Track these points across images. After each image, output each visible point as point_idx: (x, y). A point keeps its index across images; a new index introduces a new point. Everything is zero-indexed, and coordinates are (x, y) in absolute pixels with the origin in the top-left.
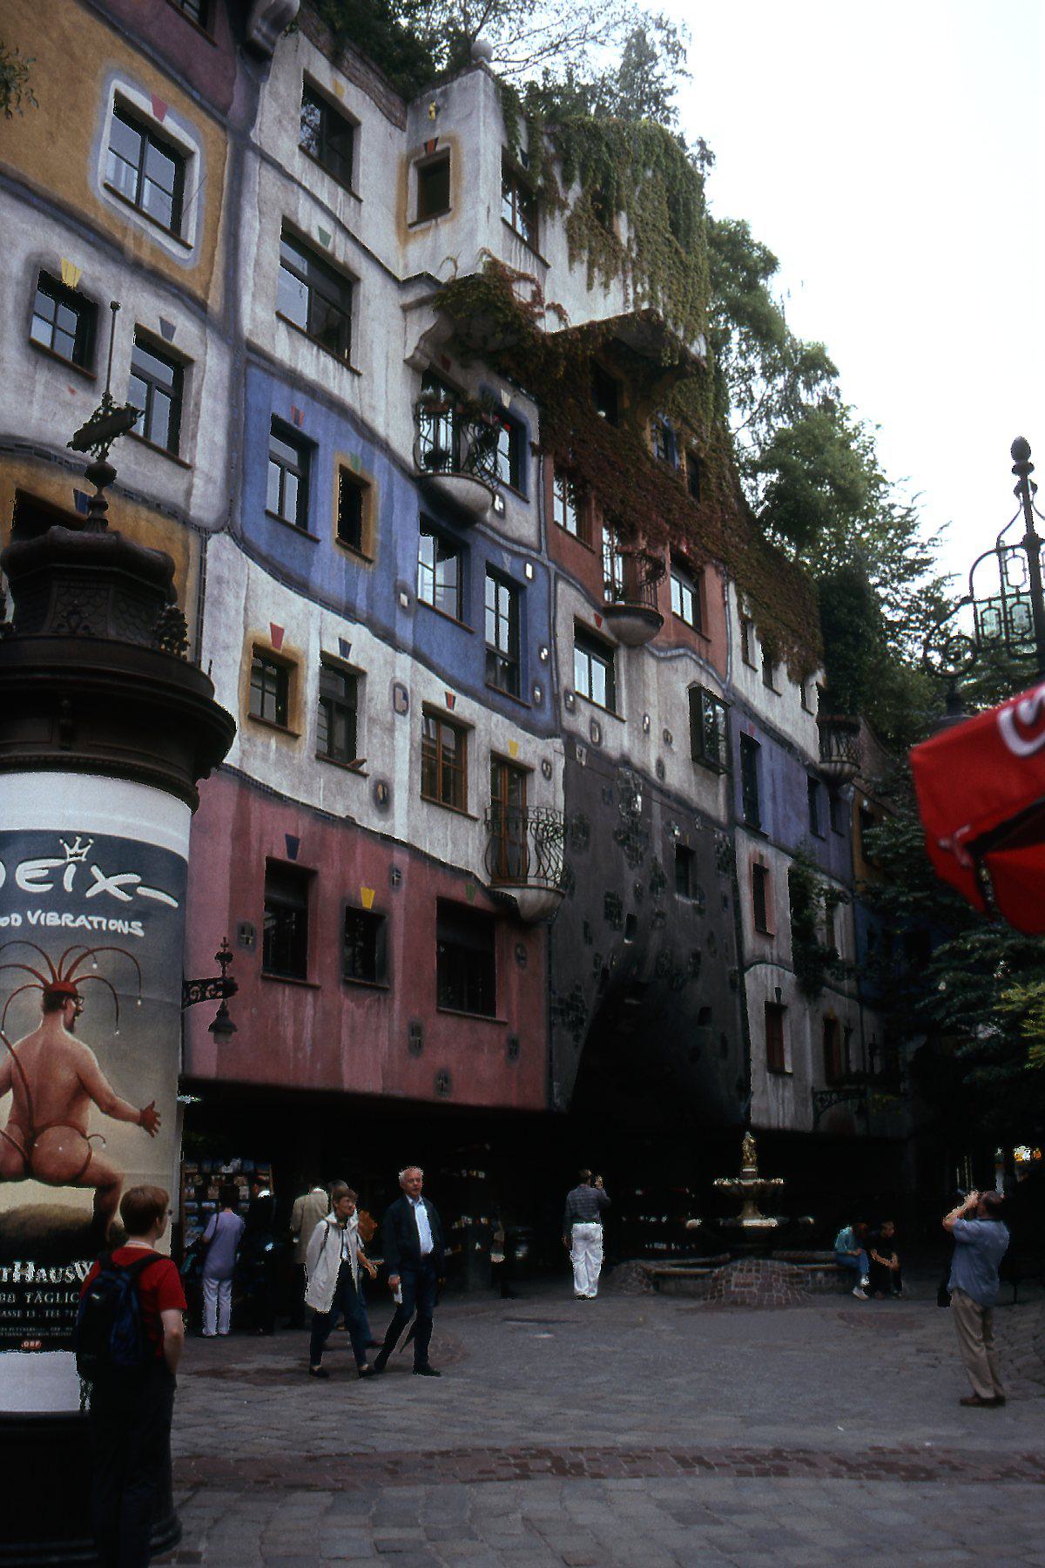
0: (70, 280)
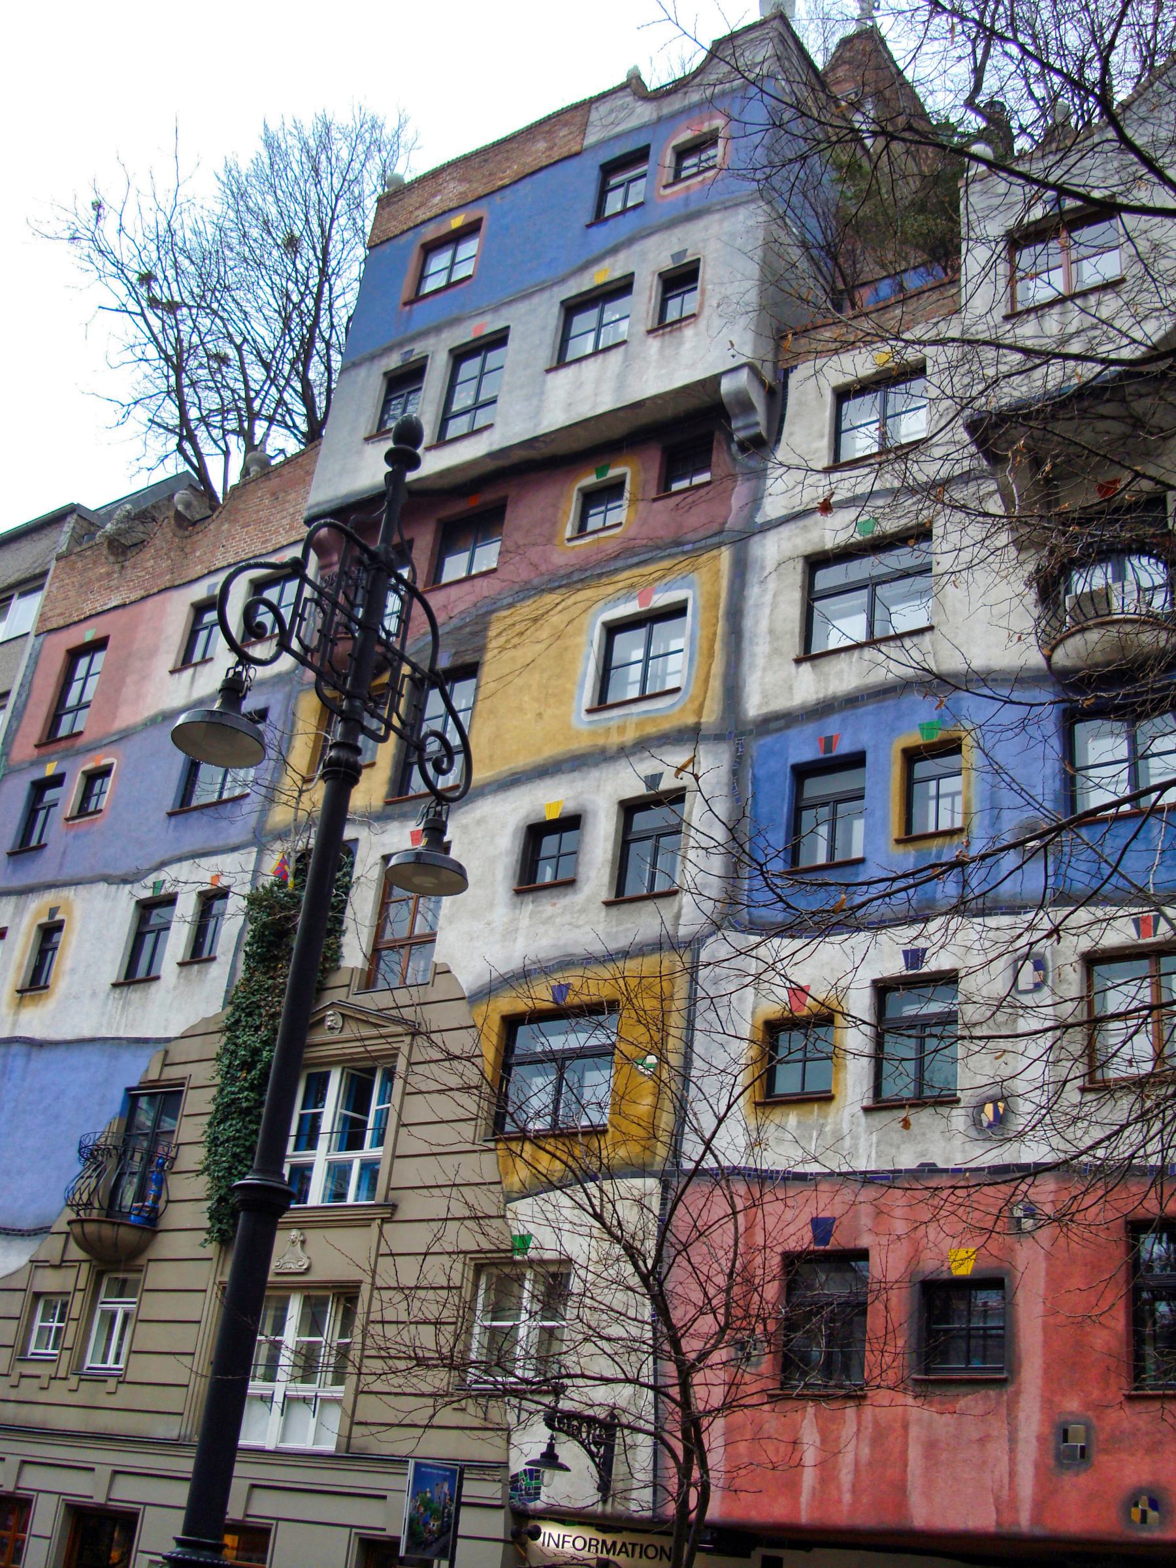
0: (552, 815)
